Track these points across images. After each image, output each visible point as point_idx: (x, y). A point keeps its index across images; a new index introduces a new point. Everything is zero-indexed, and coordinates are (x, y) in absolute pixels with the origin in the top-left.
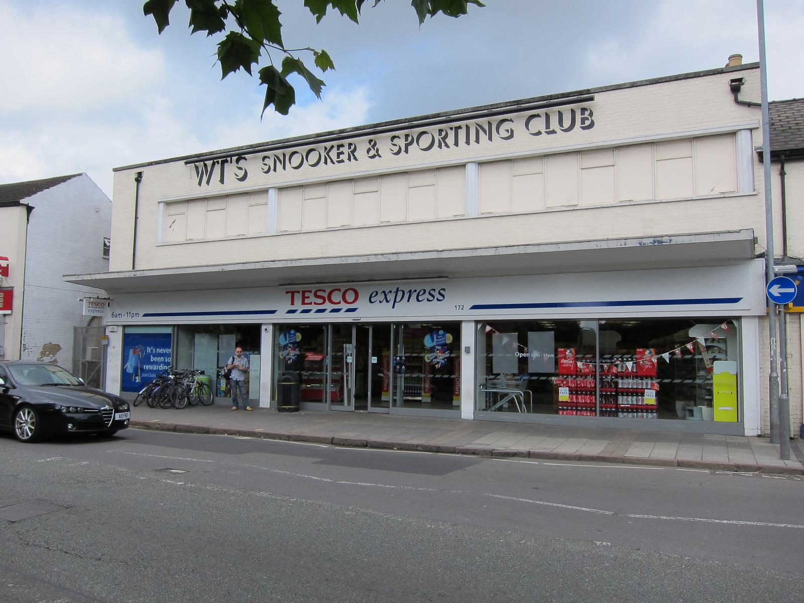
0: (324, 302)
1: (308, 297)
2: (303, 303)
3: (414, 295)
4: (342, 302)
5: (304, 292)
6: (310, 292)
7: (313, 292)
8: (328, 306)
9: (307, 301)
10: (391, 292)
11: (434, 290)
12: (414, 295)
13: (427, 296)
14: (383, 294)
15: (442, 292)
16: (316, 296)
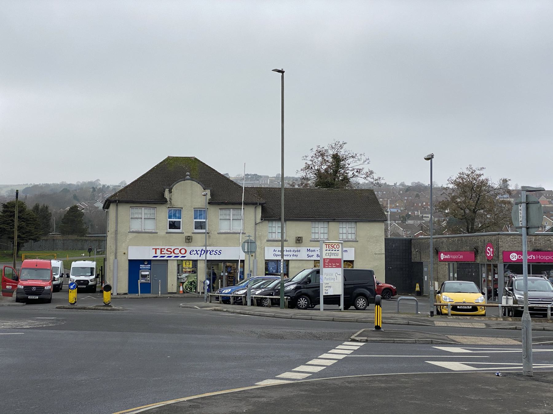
0: (171, 253)
1: (164, 251)
2: (161, 253)
3: (209, 252)
4: (179, 253)
5: (161, 249)
6: (165, 249)
7: (166, 249)
8: (173, 255)
9: (163, 253)
10: (199, 250)
11: (217, 251)
12: (209, 252)
13: (214, 252)
14: (196, 251)
15: (220, 251)
16: (167, 250)
